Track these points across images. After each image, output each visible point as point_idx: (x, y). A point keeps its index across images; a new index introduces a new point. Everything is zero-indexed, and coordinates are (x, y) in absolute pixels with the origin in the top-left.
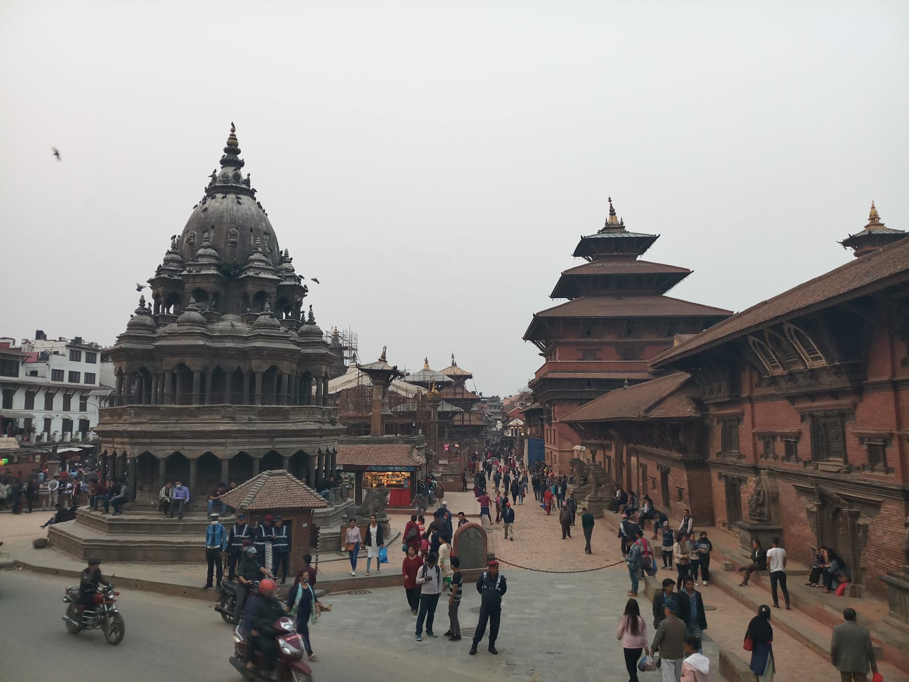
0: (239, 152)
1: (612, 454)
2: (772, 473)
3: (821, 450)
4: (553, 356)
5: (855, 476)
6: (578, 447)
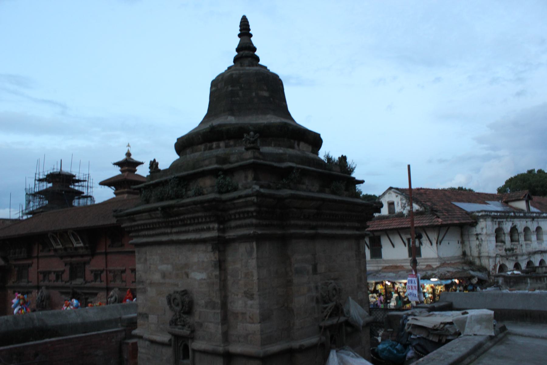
2: (47, 288)
3: (73, 276)
5: (88, 285)
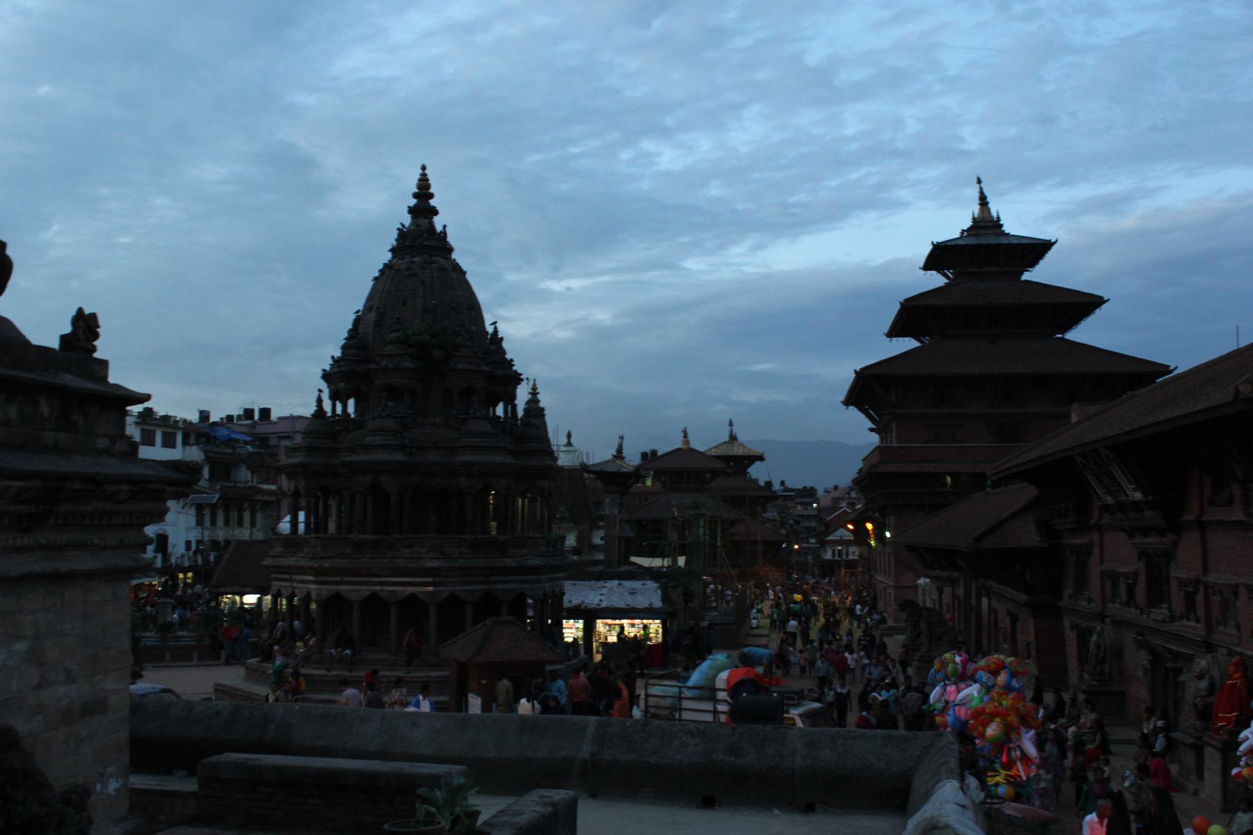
0: (431, 196)
1: (960, 592)
2: (1117, 623)
4: (889, 435)
5: (1177, 626)
6: (921, 581)
